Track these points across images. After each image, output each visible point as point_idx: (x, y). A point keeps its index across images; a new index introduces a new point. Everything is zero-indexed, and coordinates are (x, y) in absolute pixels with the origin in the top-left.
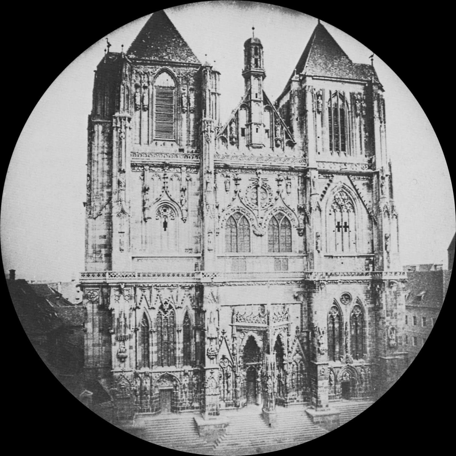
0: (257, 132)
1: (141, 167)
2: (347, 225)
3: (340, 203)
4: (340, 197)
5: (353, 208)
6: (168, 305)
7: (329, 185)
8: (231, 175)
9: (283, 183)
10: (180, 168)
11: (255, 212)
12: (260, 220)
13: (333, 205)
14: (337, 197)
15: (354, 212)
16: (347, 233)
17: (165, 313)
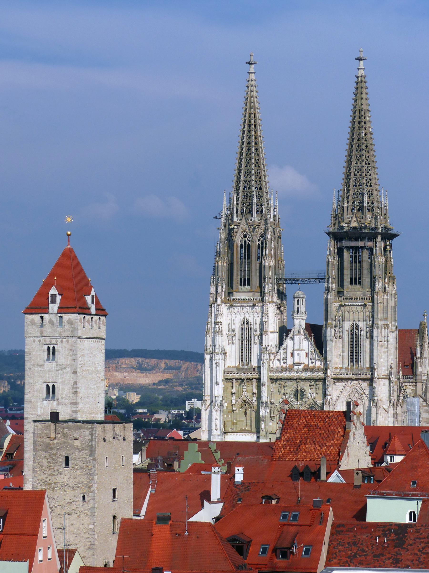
0: (298, 355)
7: (344, 387)
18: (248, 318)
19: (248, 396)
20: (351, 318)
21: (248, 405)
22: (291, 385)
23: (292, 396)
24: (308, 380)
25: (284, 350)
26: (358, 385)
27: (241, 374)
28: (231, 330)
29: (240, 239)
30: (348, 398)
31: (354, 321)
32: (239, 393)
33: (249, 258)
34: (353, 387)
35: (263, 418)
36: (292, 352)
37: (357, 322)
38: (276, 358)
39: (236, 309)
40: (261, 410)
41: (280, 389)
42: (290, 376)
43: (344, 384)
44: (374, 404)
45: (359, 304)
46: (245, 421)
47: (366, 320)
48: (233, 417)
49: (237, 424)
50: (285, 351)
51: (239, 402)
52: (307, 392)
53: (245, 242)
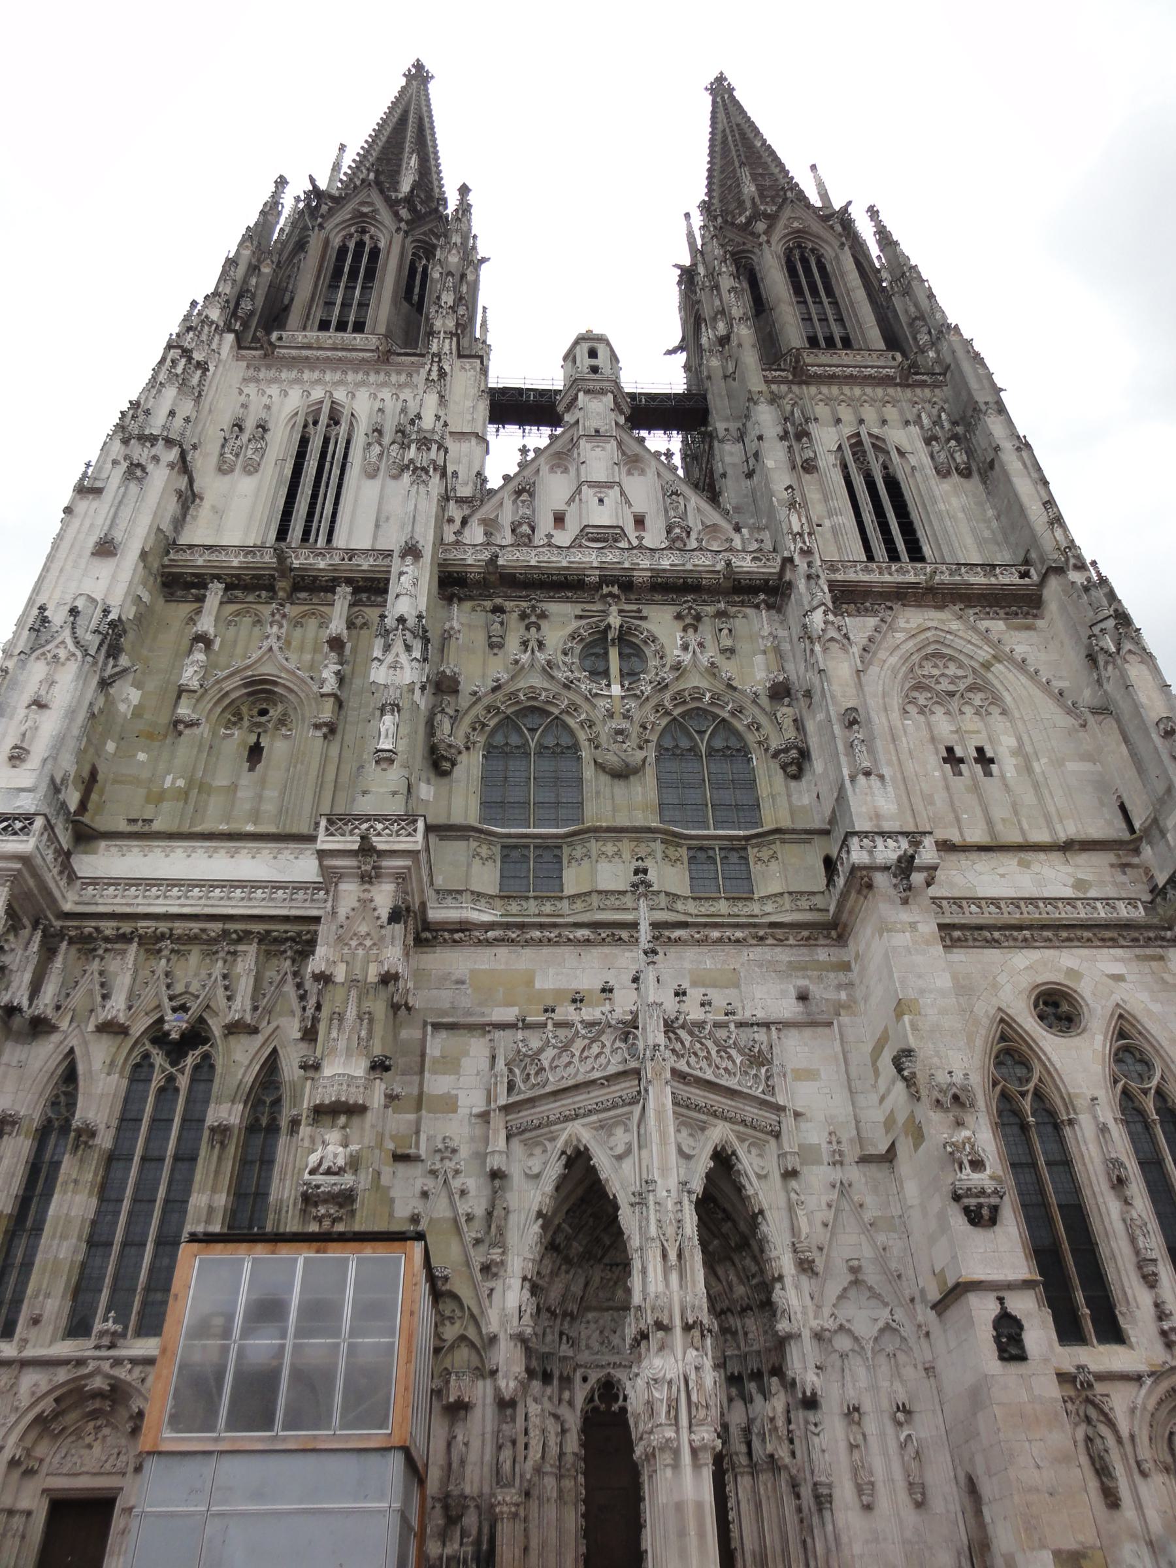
3: (938, 687)
4: (936, 672)
5: (996, 700)
12: (618, 723)
13: (916, 694)
15: (1004, 713)
20: (845, 413)
22: (566, 615)
26: (955, 626)
28: (250, 425)
29: (344, 233)
30: (907, 686)
32: (239, 650)
34: (929, 634)
35: (392, 695)
36: (560, 506)
37: (875, 431)
38: (479, 515)
40: (377, 653)
41: (497, 626)
42: (565, 564)
43: (872, 621)
47: (918, 421)
49: (184, 794)
51: (228, 686)
52: (663, 639)
53: (360, 245)
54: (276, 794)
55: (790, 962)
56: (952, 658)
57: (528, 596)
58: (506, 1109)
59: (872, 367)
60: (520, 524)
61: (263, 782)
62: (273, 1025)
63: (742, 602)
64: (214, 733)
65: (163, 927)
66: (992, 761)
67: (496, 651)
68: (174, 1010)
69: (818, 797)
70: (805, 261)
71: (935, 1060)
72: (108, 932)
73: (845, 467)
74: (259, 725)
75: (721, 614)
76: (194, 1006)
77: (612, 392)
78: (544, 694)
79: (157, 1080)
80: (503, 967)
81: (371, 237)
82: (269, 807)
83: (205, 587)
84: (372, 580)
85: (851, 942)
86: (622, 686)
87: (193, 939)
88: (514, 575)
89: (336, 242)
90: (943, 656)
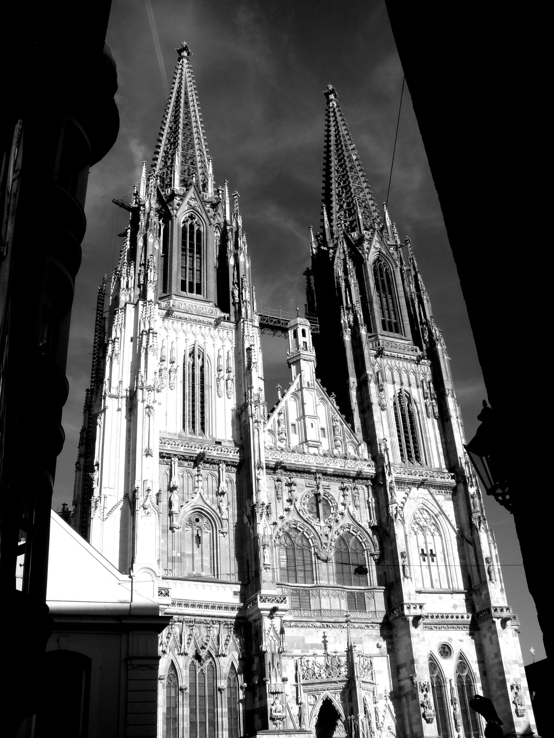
0: (312, 426)
1: (168, 458)
2: (434, 553)
3: (421, 523)
4: (420, 516)
5: (438, 530)
6: (206, 651)
8: (283, 478)
9: (349, 493)
10: (218, 464)
11: (317, 528)
13: (413, 526)
14: (416, 516)
15: (440, 535)
16: (435, 564)
17: (202, 665)
18: (202, 345)
19: (210, 498)
20: (397, 379)
21: (205, 520)
22: (302, 485)
23: (306, 507)
24: (338, 476)
25: (280, 414)
26: (430, 497)
27: (193, 448)
28: (168, 359)
31: (402, 384)
32: (185, 491)
33: (199, 252)
35: (267, 540)
36: (295, 422)
37: (407, 389)
39: (177, 325)
40: (258, 520)
42: (304, 463)
44: (482, 526)
45: (408, 357)
46: (197, 558)
48: (170, 546)
50: (282, 417)
52: (337, 501)
53: (192, 226)
54: (208, 559)
55: (376, 635)
56: (426, 511)
57: (289, 475)
58: (303, 685)
59: (408, 355)
60: (282, 433)
61: (202, 553)
62: (231, 654)
63: (363, 483)
64: (183, 530)
65: (193, 618)
66: (434, 555)
67: (280, 501)
68: (202, 648)
69: (385, 573)
70: (381, 270)
71: (422, 677)
72: (175, 620)
73: (395, 404)
74: (198, 527)
75: (355, 488)
76: (208, 648)
77: (314, 361)
78: (299, 523)
79: (198, 671)
80: (294, 635)
81: (196, 223)
82: (207, 564)
83: (170, 458)
84: (233, 462)
85: (394, 630)
86: (324, 521)
87: (200, 623)
88: (286, 466)
89: (182, 225)
90: (424, 509)
